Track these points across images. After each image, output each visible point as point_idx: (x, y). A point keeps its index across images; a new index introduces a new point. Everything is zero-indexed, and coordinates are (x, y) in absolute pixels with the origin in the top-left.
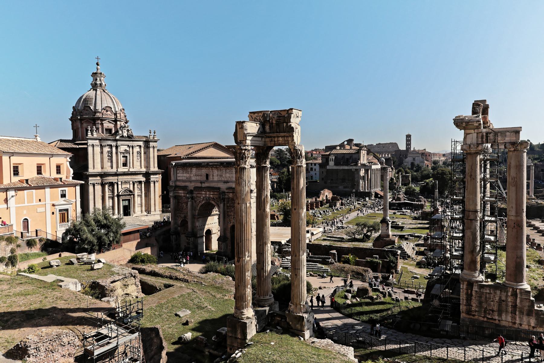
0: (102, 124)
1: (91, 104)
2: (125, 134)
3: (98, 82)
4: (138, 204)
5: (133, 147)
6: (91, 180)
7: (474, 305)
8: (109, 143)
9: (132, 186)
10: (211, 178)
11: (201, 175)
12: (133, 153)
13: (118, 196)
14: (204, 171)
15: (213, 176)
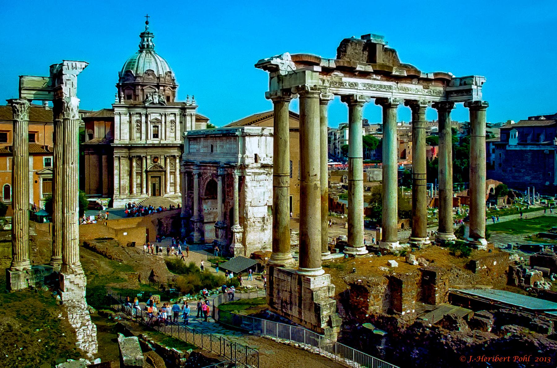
0: (143, 90)
1: (132, 69)
2: (156, 101)
3: (145, 44)
4: (171, 183)
5: (165, 115)
6: (117, 153)
7: (275, 295)
8: (138, 110)
9: (163, 161)
10: (214, 149)
11: (207, 147)
12: (165, 123)
13: (147, 172)
14: (210, 142)
15: (216, 146)
